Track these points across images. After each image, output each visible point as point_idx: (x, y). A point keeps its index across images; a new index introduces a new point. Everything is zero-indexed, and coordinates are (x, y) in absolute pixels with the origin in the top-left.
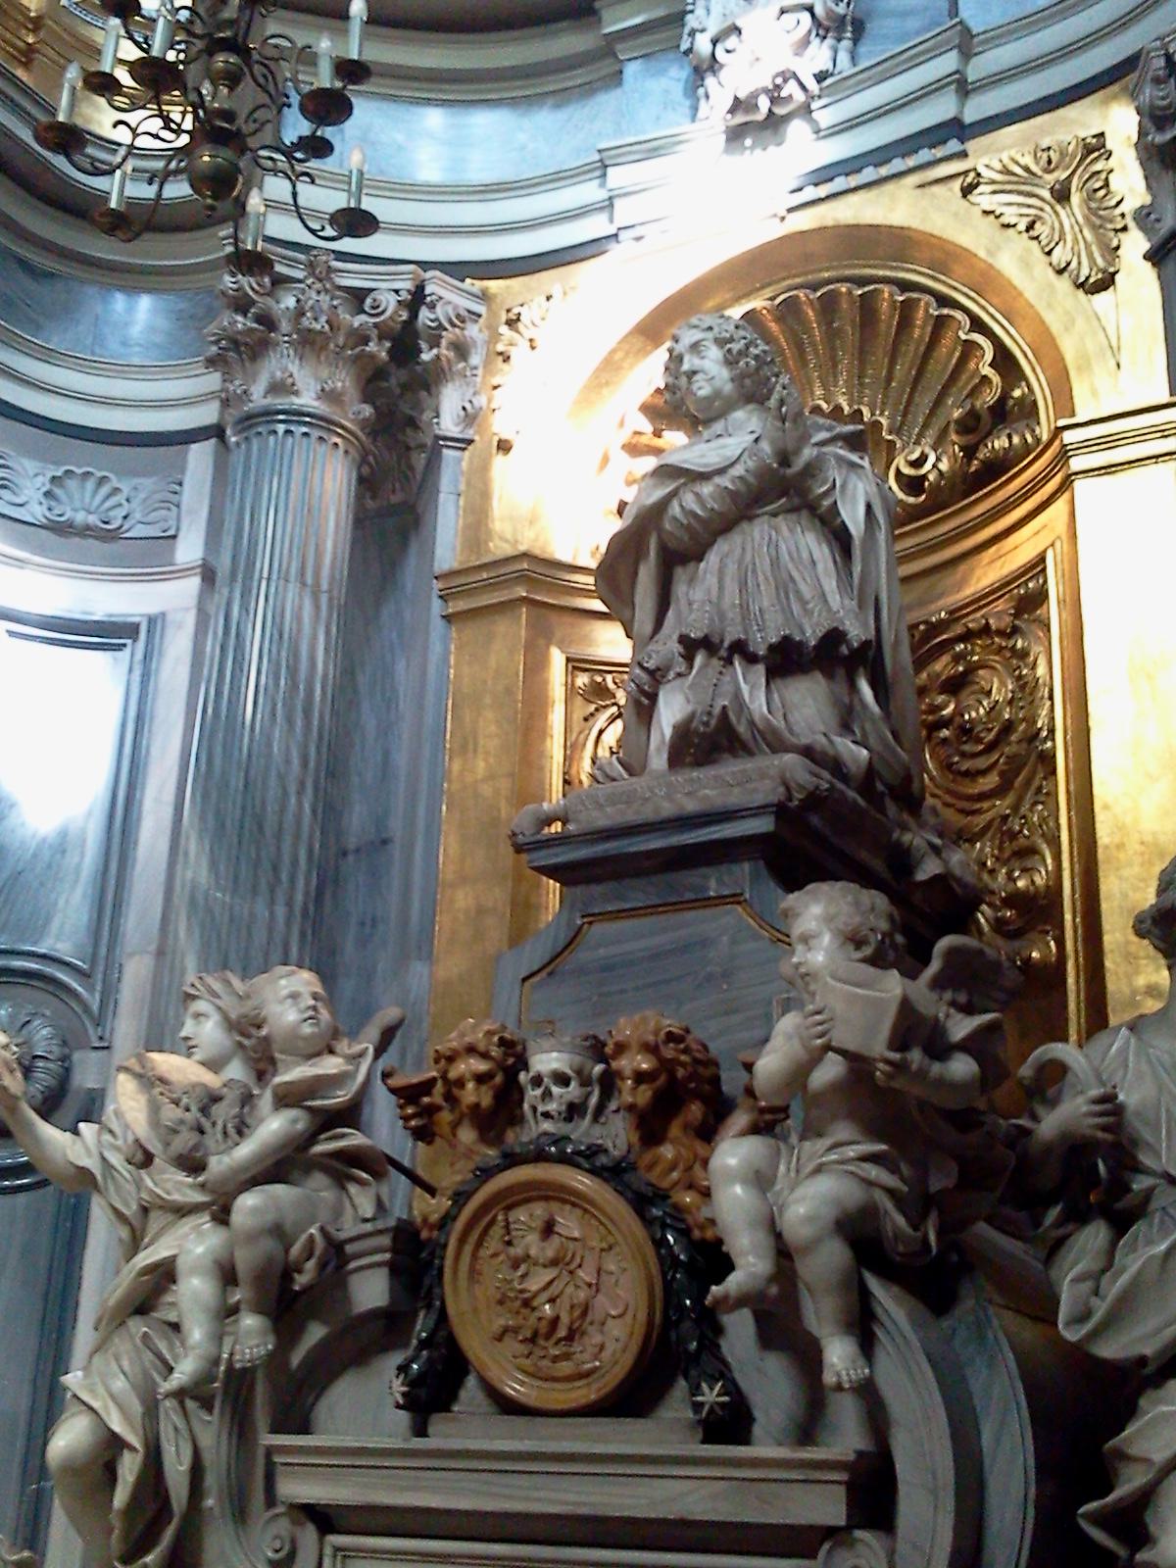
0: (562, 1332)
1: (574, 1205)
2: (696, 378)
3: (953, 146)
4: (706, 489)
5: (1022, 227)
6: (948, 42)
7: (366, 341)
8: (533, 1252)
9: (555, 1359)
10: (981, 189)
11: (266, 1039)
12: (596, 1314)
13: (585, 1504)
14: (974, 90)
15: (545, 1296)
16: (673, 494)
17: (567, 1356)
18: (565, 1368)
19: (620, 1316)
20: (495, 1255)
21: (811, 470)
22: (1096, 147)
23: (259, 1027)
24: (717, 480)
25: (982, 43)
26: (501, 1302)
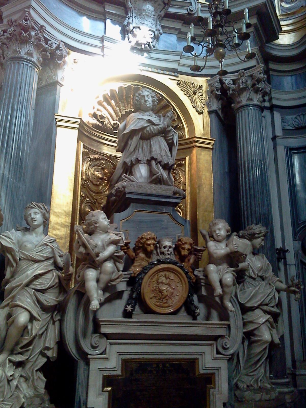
0: (167, 298)
1: (173, 273)
2: (147, 102)
3: (176, 74)
4: (155, 127)
5: (188, 96)
6: (179, 54)
7: (47, 51)
8: (164, 281)
9: (165, 303)
10: (180, 85)
11: (96, 227)
12: (174, 295)
13: (176, 332)
14: (180, 65)
15: (165, 291)
16: (149, 126)
17: (166, 303)
18: (166, 305)
19: (179, 295)
20: (154, 281)
21: (170, 131)
22: (201, 87)
23: (96, 223)
24: (157, 126)
25: (183, 57)
26: (153, 291)
